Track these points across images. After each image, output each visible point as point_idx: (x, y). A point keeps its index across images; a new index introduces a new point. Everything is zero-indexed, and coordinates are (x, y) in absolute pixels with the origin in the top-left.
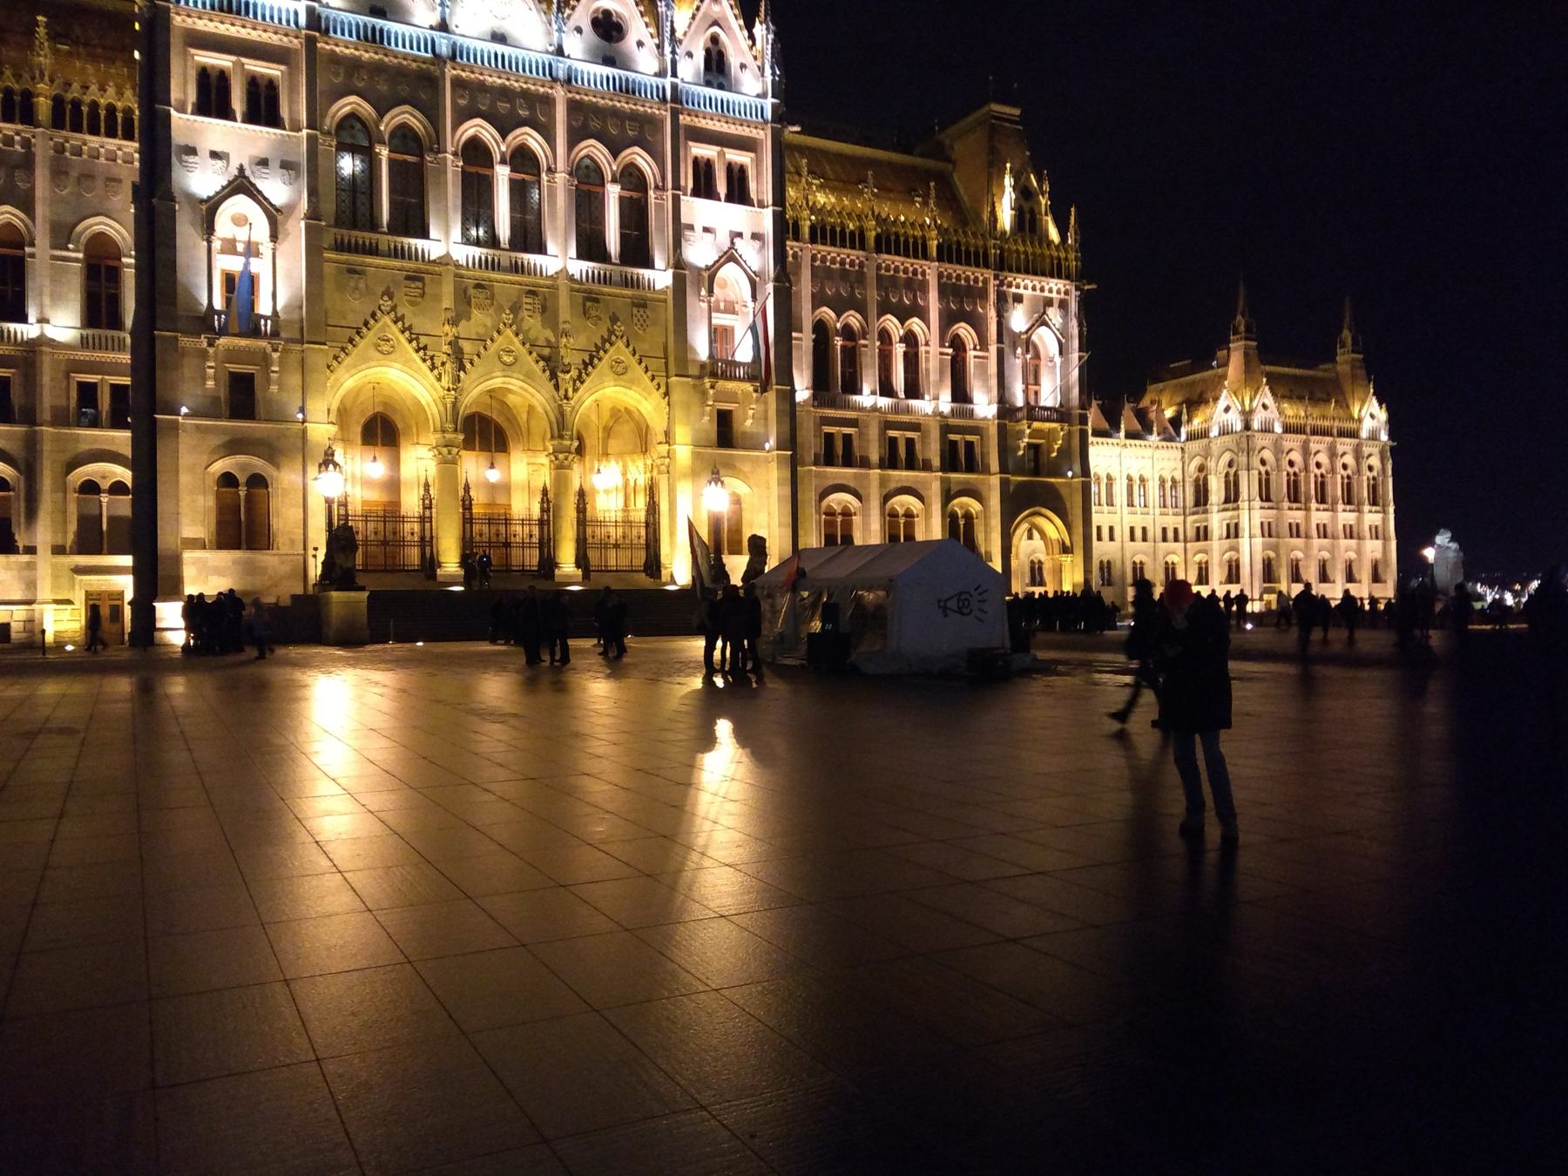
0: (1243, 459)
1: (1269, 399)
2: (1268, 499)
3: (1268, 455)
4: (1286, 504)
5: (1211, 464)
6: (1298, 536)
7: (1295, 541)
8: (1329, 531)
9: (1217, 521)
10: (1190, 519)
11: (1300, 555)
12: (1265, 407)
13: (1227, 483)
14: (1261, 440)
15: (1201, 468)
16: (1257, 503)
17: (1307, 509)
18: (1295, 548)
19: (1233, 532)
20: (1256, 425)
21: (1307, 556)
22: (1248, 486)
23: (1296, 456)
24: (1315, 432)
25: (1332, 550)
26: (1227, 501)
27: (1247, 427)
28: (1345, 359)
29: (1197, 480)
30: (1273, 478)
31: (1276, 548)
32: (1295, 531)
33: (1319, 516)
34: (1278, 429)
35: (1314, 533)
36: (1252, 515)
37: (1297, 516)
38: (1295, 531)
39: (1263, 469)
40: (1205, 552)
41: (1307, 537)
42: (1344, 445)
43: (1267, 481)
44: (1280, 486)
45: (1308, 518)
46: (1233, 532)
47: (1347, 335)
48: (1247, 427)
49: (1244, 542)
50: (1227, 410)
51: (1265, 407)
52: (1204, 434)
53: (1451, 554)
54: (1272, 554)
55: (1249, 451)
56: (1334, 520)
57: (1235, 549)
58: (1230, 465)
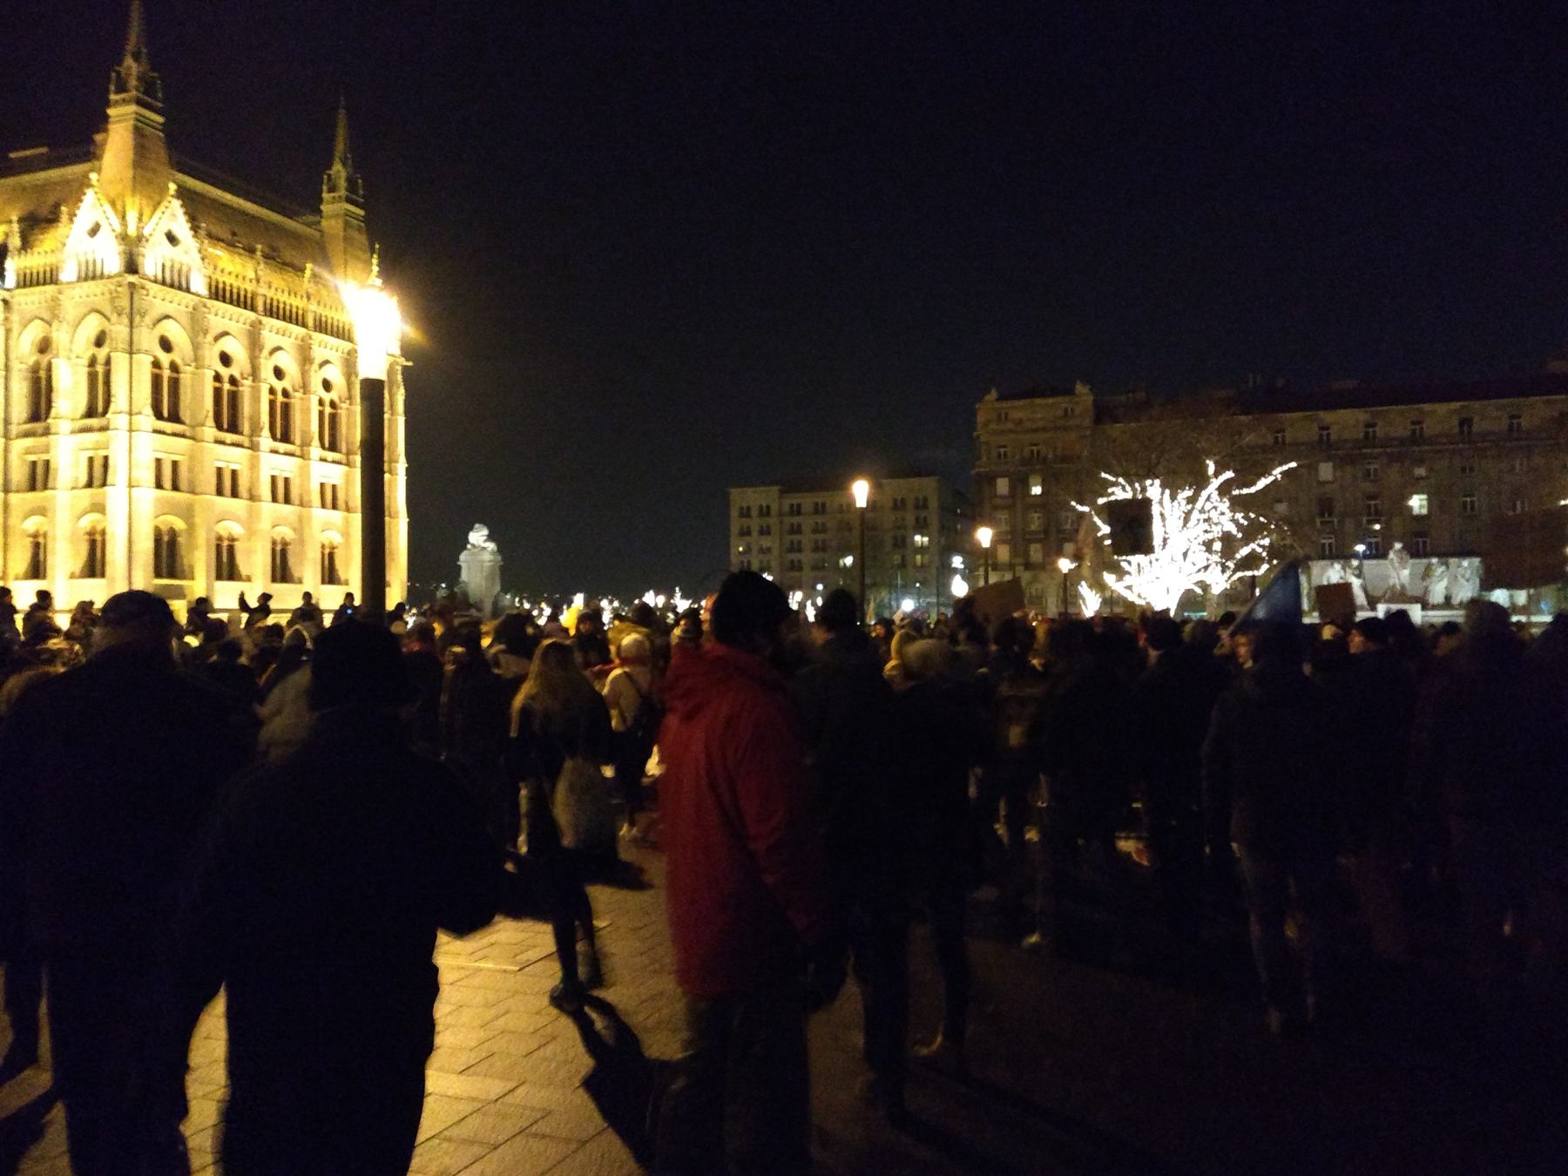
0: (119, 330)
1: (182, 228)
2: (175, 417)
3: (173, 330)
4: (210, 431)
5: (60, 336)
6: (235, 494)
7: (227, 503)
8: (295, 493)
9: (68, 451)
10: (18, 445)
11: (236, 529)
12: (172, 239)
13: (92, 377)
14: (159, 300)
15: (44, 346)
16: (147, 420)
17: (254, 447)
18: (228, 517)
19: (98, 474)
20: (150, 264)
21: (251, 533)
22: (132, 386)
23: (237, 348)
24: (272, 311)
25: (300, 527)
26: (91, 413)
27: (132, 267)
28: (335, 209)
29: (35, 370)
30: (186, 378)
31: (188, 514)
32: (228, 485)
33: (274, 462)
34: (199, 285)
35: (265, 491)
36: (136, 441)
37: (234, 458)
38: (228, 485)
39: (165, 359)
40: (42, 511)
41: (253, 497)
42: (324, 347)
43: (175, 384)
44: (199, 397)
45: (254, 466)
46: (98, 474)
47: (339, 170)
48: (132, 267)
49: (115, 495)
50: (94, 231)
51: (172, 239)
52: (49, 278)
53: (487, 557)
54: (179, 525)
55: (133, 316)
56: (305, 473)
57: (99, 508)
58: (99, 342)
